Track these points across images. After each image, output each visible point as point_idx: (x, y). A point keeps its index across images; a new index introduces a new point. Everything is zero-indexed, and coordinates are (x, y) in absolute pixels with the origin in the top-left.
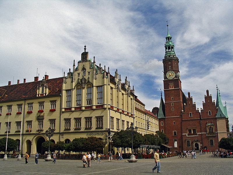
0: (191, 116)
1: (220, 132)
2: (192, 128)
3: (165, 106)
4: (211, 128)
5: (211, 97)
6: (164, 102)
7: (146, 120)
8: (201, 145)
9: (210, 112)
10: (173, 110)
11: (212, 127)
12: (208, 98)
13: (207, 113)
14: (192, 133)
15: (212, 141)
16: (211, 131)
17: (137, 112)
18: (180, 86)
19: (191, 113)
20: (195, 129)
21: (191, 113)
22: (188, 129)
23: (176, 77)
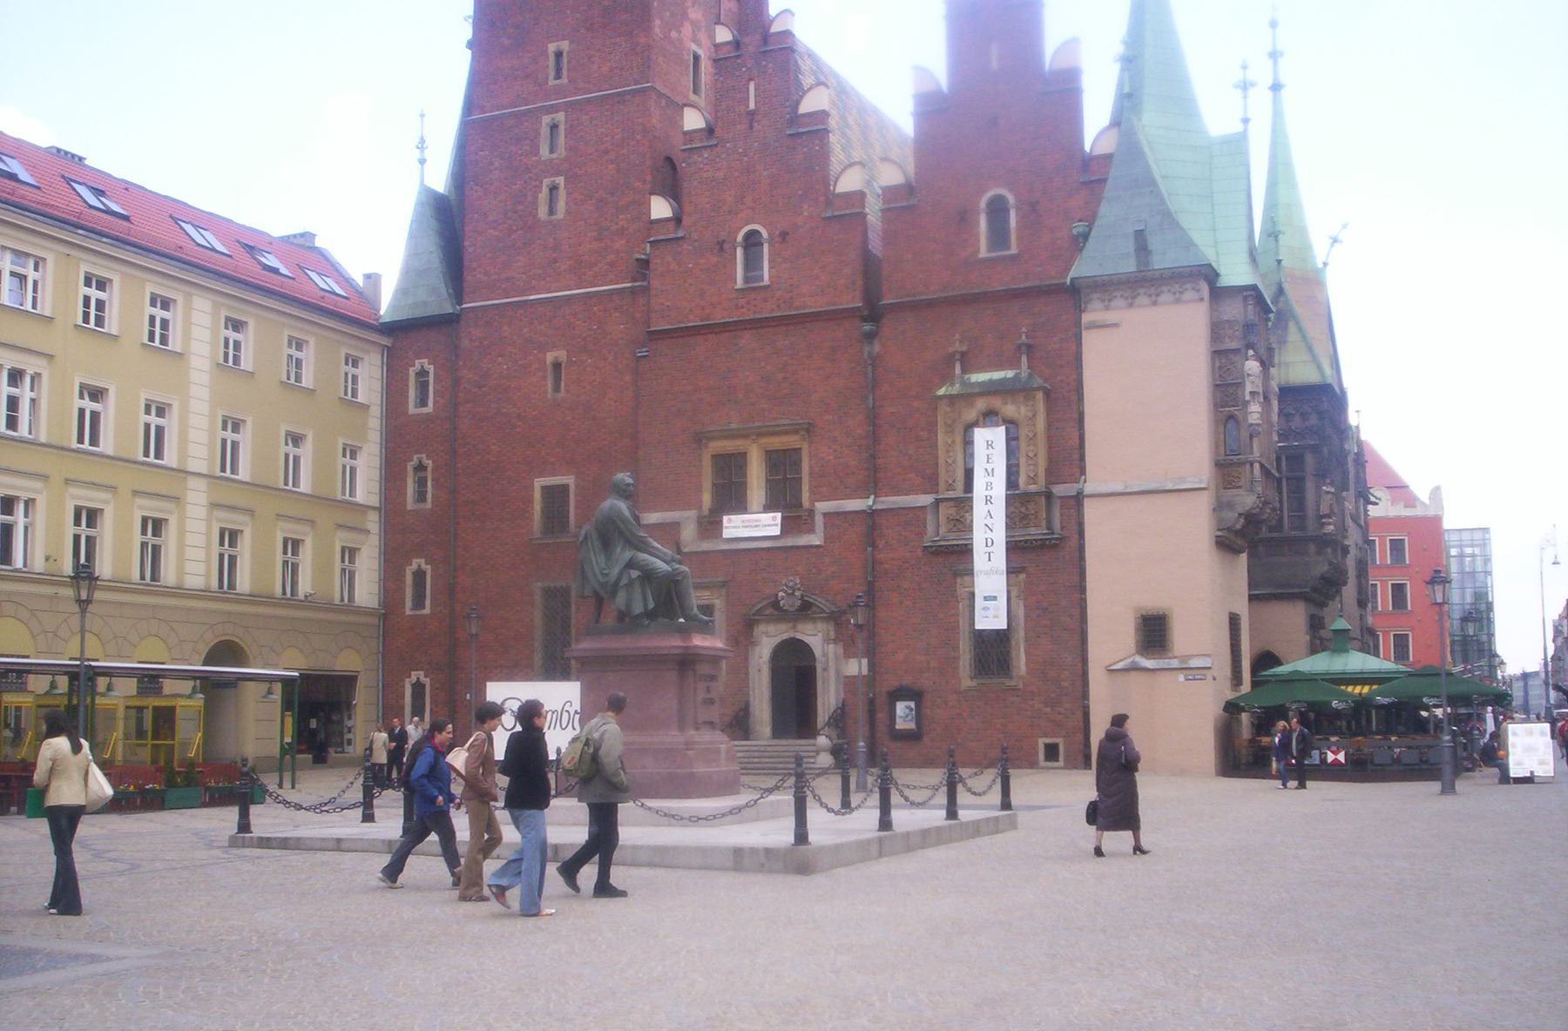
8: (856, 667)
10: (551, 212)
13: (964, 218)
20: (791, 441)
21: (752, 241)
22: (718, 446)
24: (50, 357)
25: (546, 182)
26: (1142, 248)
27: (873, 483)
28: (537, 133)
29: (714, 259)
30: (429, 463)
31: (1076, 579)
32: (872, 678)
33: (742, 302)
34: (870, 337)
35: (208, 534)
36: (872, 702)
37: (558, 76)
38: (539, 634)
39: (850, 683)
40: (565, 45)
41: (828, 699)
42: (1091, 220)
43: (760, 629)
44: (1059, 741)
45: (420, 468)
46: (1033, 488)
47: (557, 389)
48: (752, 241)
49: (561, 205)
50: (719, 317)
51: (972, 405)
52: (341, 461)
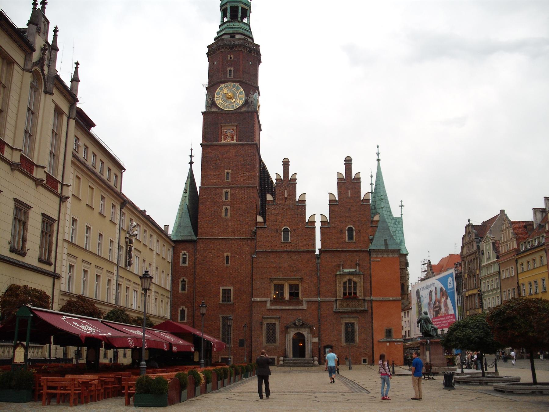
0: (286, 238)
1: (381, 298)
2: (288, 280)
3: (200, 199)
4: (350, 283)
5: (357, 180)
6: (198, 184)
7: (121, 229)
8: (316, 340)
9: (350, 230)
10: (226, 215)
11: (355, 279)
12: (348, 183)
13: (342, 231)
14: (287, 296)
15: (350, 327)
16: (350, 294)
17: (85, 183)
18: (256, 139)
19: (286, 231)
21: (286, 231)
23: (246, 103)
24: (140, 252)
26: (386, 244)
27: (318, 294)
28: (222, 194)
29: (275, 234)
30: (187, 280)
31: (370, 320)
32: (319, 344)
36: (319, 349)
38: (221, 329)
39: (314, 343)
40: (230, 171)
41: (308, 348)
42: (374, 235)
44: (367, 358)
45: (184, 281)
46: (360, 298)
47: (227, 263)
49: (229, 214)
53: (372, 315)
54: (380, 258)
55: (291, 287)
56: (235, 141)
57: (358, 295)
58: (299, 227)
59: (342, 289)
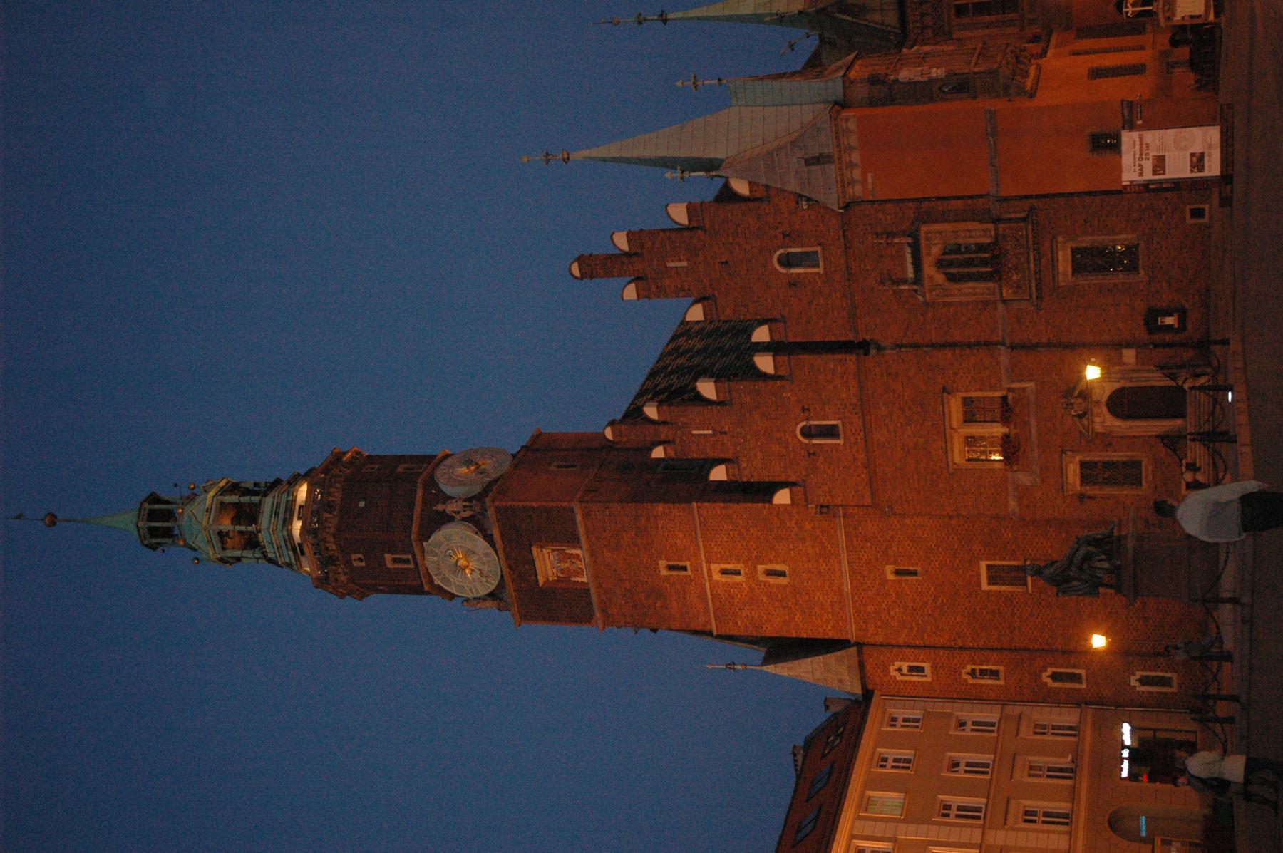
0: (830, 432)
4: (951, 264)
9: (787, 261)
10: (782, 574)
11: (936, 250)
13: (793, 283)
25: (762, 578)
30: (969, 668)
33: (853, 439)
34: (880, 348)
35: (1027, 830)
36: (1156, 346)
37: (684, 569)
43: (1098, 428)
45: (972, 673)
47: (915, 573)
48: (807, 433)
49: (779, 567)
50: (862, 457)
51: (931, 278)
52: (968, 733)
53: (1047, 196)
54: (864, 174)
55: (969, 419)
56: (578, 552)
57: (988, 241)
58: (793, 399)
59: (968, 287)
